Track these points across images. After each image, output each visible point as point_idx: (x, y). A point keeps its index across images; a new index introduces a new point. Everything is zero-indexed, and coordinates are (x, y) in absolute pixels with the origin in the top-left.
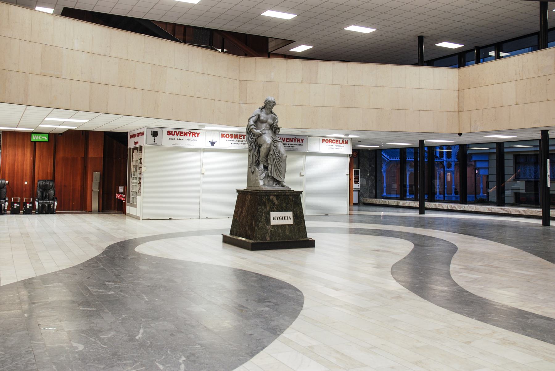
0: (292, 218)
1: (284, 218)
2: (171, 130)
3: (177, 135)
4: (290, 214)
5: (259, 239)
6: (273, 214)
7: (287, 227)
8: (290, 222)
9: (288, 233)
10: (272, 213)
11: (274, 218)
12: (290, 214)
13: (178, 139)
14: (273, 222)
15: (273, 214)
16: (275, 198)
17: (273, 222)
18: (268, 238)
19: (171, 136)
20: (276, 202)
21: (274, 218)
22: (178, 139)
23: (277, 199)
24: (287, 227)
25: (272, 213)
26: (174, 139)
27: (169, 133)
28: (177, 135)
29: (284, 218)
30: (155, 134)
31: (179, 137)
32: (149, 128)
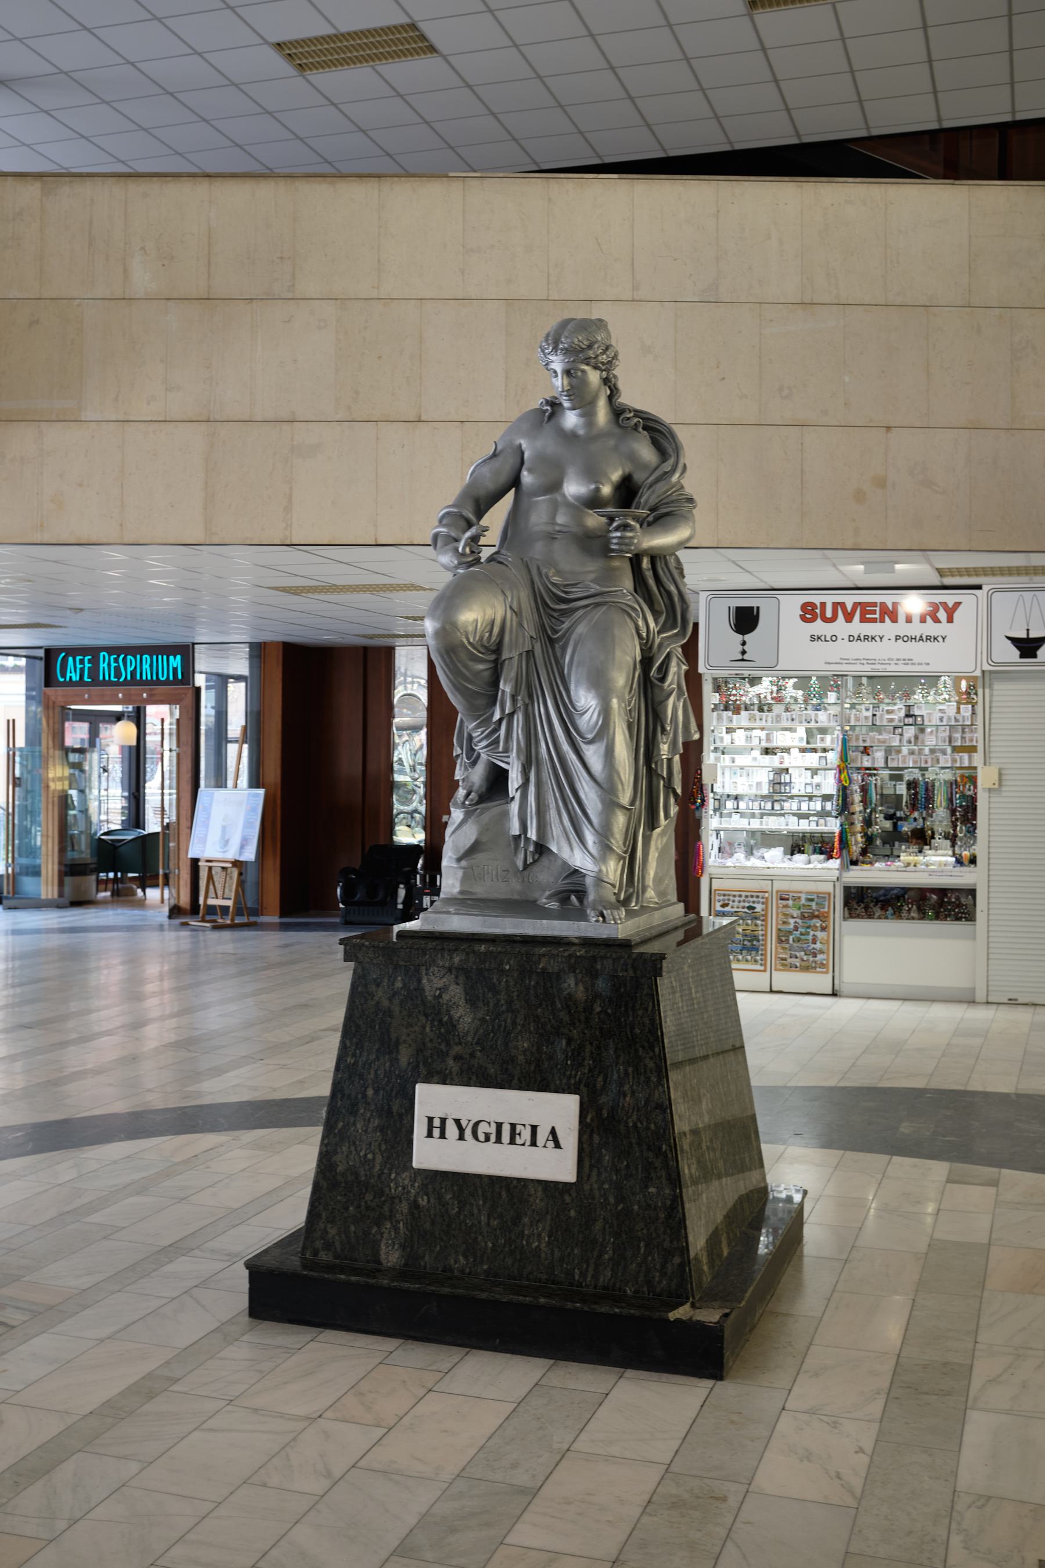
0: (570, 1139)
1: (506, 1133)
2: (816, 598)
3: (849, 618)
4: (560, 1110)
5: (328, 1246)
6: (431, 1099)
7: (538, 1201)
8: (560, 1166)
9: (538, 1238)
10: (421, 1090)
11: (437, 1128)
12: (560, 1110)
13: (851, 638)
14: (428, 1154)
15: (431, 1099)
16: (455, 993)
17: (428, 1154)
18: (391, 1256)
19: (819, 627)
20: (465, 1018)
21: (437, 1128)
22: (851, 638)
23: (472, 1001)
24: (538, 1201)
25: (421, 1090)
26: (834, 638)
27: (809, 612)
28: (849, 618)
29: (506, 1133)
30: (746, 620)
31: (857, 627)
32: (719, 593)
